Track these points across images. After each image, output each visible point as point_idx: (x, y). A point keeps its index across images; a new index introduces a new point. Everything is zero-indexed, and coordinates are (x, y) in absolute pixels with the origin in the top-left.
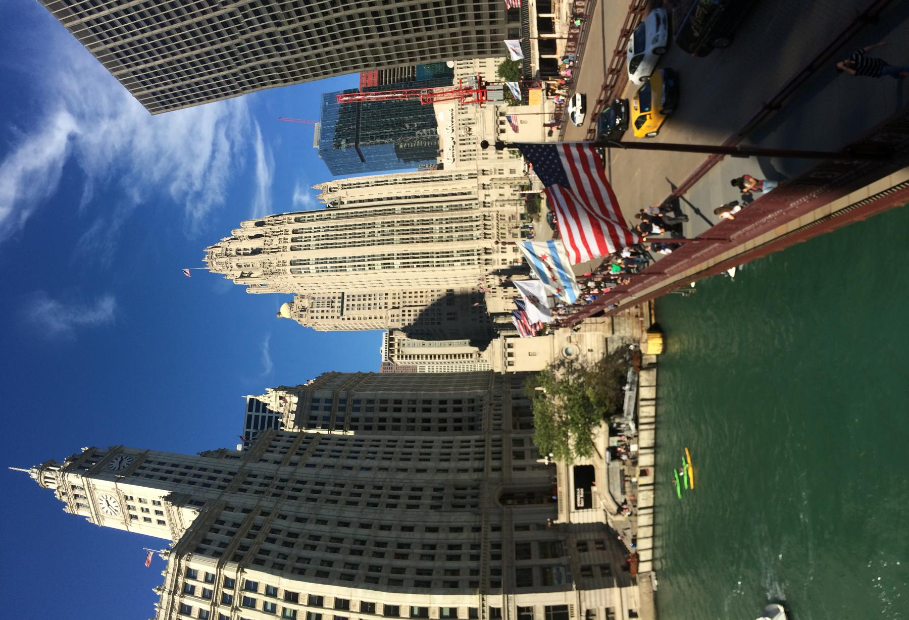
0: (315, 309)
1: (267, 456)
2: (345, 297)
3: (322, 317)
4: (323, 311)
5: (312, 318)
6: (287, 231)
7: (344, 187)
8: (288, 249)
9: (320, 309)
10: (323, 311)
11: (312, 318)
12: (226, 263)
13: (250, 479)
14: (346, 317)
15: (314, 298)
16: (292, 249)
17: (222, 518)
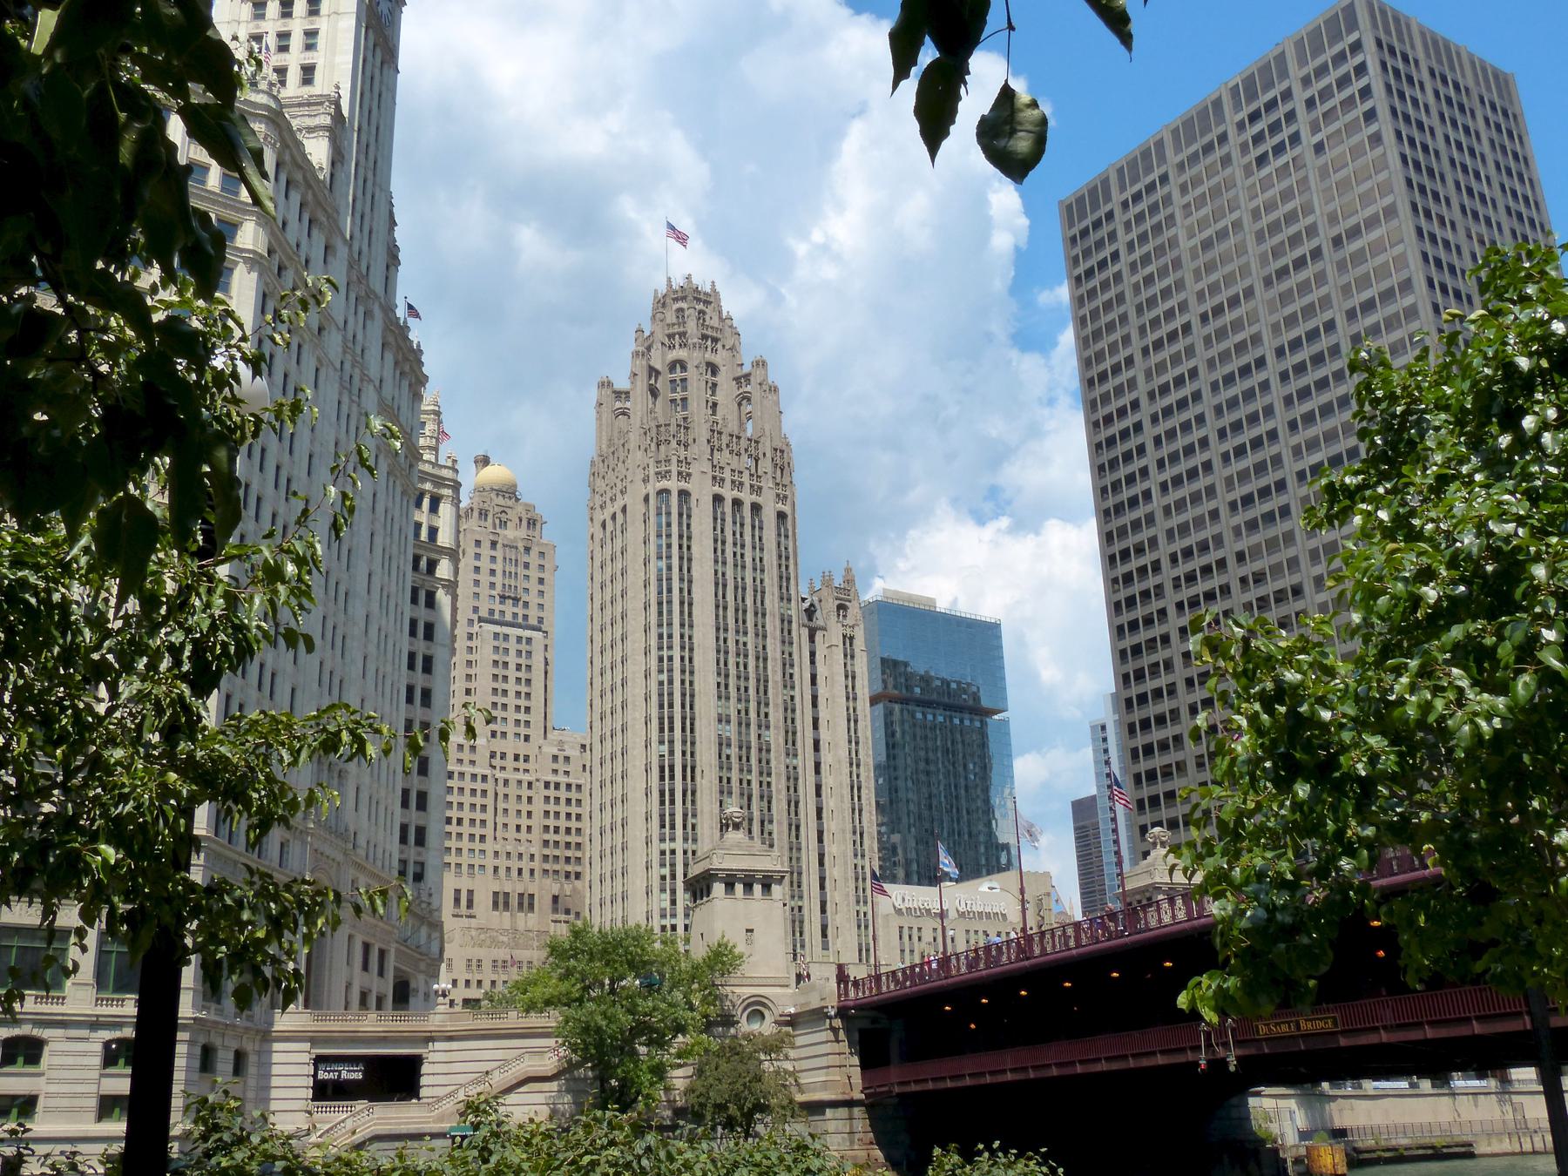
0: (499, 554)
1: (389, 357)
2: (528, 633)
3: (477, 569)
4: (493, 572)
5: (478, 543)
6: (758, 490)
7: (849, 639)
8: (717, 489)
9: (498, 567)
10: (493, 572)
11: (478, 543)
12: (683, 334)
13: (361, 310)
14: (476, 628)
15: (527, 549)
16: (718, 499)
17: (315, 232)
